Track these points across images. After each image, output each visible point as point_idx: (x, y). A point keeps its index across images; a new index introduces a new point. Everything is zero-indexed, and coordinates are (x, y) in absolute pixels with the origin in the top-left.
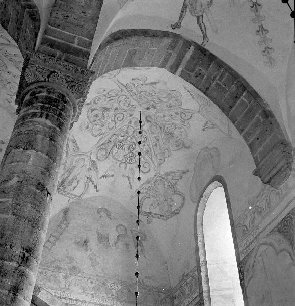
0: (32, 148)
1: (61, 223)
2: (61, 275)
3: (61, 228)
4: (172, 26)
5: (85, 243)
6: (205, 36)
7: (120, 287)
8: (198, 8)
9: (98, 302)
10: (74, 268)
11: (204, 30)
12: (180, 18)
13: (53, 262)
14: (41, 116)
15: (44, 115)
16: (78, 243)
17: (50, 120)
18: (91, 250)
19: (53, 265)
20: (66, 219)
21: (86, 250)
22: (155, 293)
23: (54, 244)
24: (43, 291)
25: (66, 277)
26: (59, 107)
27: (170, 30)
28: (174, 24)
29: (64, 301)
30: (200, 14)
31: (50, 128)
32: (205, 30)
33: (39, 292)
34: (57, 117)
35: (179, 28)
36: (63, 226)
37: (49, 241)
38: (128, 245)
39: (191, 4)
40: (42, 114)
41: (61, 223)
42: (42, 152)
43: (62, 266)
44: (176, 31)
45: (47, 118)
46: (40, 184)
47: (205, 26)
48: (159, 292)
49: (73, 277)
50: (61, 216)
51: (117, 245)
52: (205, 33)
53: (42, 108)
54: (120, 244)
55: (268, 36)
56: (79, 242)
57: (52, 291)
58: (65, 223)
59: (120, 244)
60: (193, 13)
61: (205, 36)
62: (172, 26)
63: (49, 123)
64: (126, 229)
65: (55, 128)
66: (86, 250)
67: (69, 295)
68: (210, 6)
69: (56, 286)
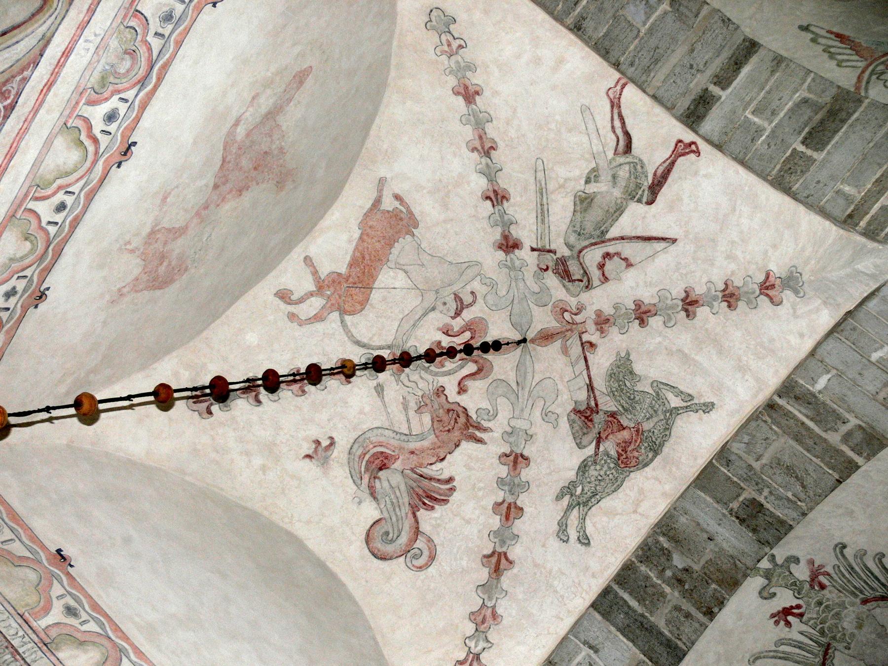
4: (698, 153)
6: (615, 104)
8: (624, 173)
11: (616, 117)
12: (673, 163)
27: (702, 145)
28: (692, 156)
30: (622, 160)
32: (612, 119)
35: (680, 141)
39: (638, 186)
44: (688, 136)
47: (613, 127)
52: (616, 111)
55: (452, 81)
60: (638, 167)
61: (615, 104)
62: (698, 153)
68: (593, 170)
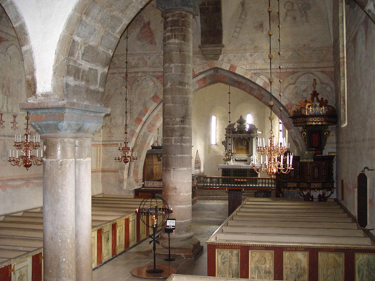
0: (172, 63)
1: (241, 15)
2: (248, 54)
3: (242, 19)
5: (261, 26)
7: (291, 53)
9: (276, 67)
10: (256, 47)
13: (241, 47)
14: (172, 38)
15: (173, 36)
16: (256, 27)
17: (177, 38)
18: (266, 30)
19: (242, 49)
20: (244, 11)
21: (263, 31)
22: (318, 52)
23: (239, 33)
24: (238, 68)
25: (251, 55)
26: (180, 25)
29: (253, 71)
31: (178, 44)
33: (236, 69)
34: (180, 34)
36: (243, 17)
37: (235, 32)
38: (294, 18)
40: (172, 35)
41: (241, 14)
42: (177, 63)
43: (247, 48)
45: (175, 38)
46: (180, 82)
48: (321, 50)
49: (256, 54)
50: (240, 9)
51: (286, 20)
53: (171, 31)
54: (288, 18)
56: (257, 26)
57: (244, 67)
58: (244, 14)
59: (288, 18)
63: (177, 41)
64: (293, 4)
65: (181, 43)
66: (263, 31)
67: (255, 67)
69: (245, 63)
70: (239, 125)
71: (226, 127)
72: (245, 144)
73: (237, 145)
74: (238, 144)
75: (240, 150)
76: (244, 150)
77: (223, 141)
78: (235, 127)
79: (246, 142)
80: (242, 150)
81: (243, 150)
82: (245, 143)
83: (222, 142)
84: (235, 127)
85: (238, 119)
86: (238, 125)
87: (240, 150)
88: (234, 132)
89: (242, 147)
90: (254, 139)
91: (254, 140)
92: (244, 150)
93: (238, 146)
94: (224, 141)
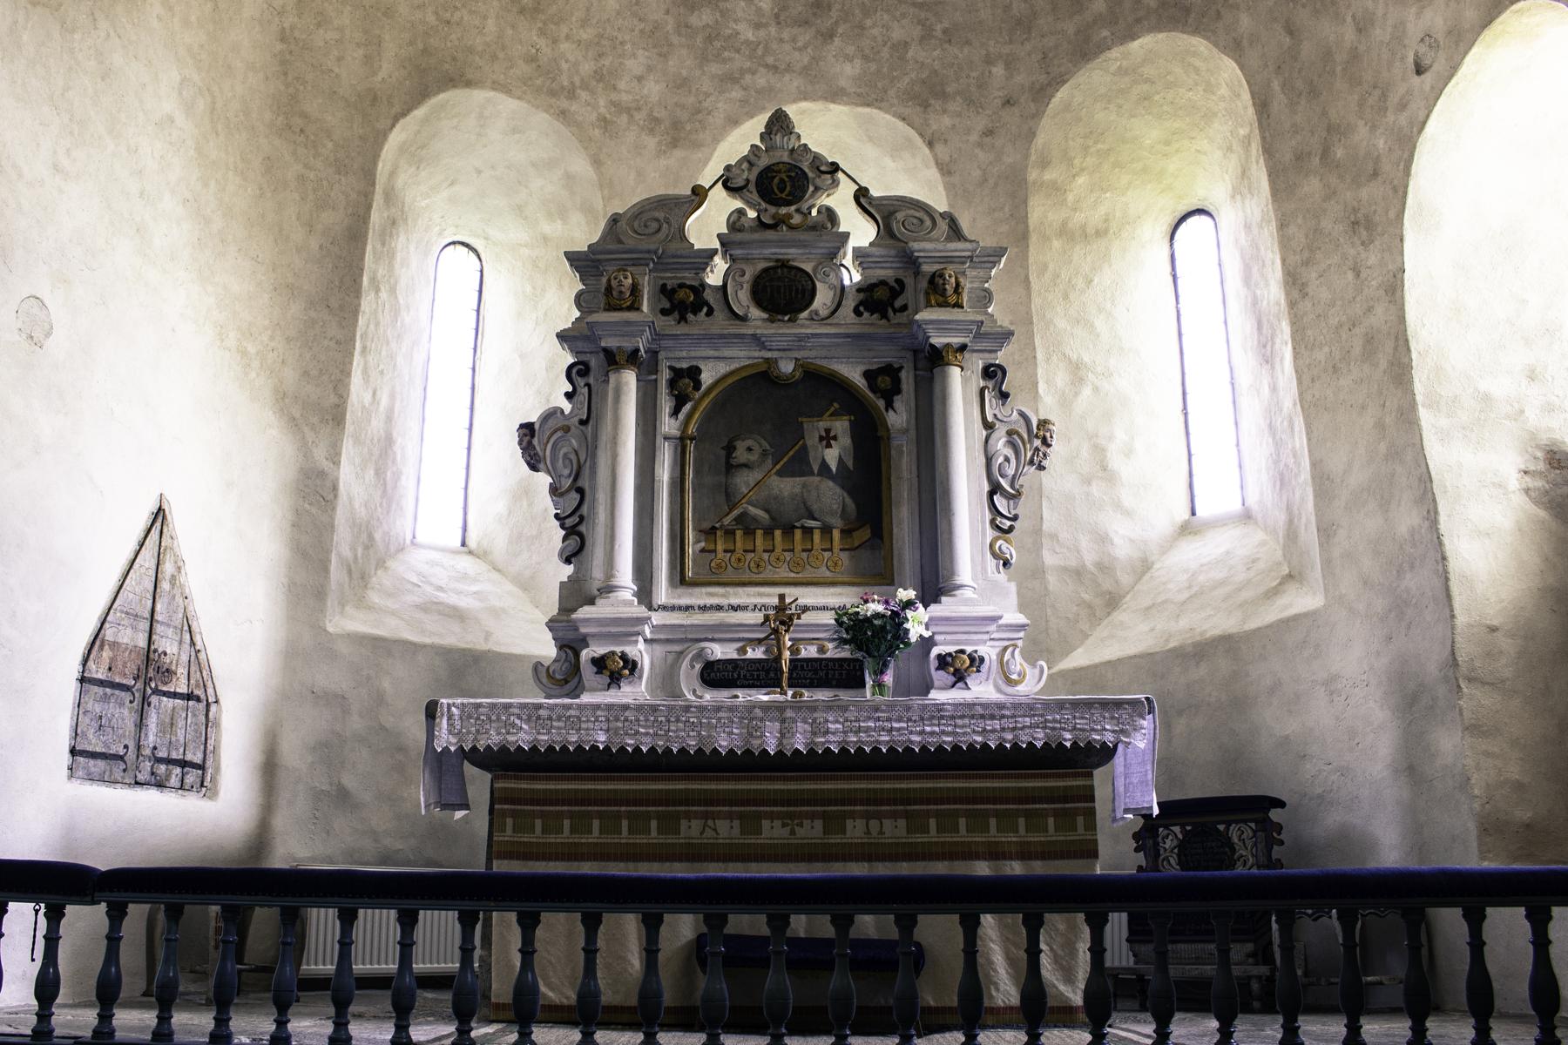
70: (752, 214)
71: (585, 234)
72: (832, 456)
73: (730, 467)
74: (741, 455)
75: (769, 532)
76: (826, 530)
77: (533, 418)
78: (705, 227)
79: (841, 426)
80: (789, 530)
81: (808, 532)
82: (828, 439)
83: (527, 430)
84: (705, 227)
85: (745, 150)
86: (741, 212)
87: (769, 532)
88: (685, 300)
89: (787, 487)
90: (955, 372)
91: (960, 385)
92: (826, 530)
93: (744, 482)
94: (551, 414)
